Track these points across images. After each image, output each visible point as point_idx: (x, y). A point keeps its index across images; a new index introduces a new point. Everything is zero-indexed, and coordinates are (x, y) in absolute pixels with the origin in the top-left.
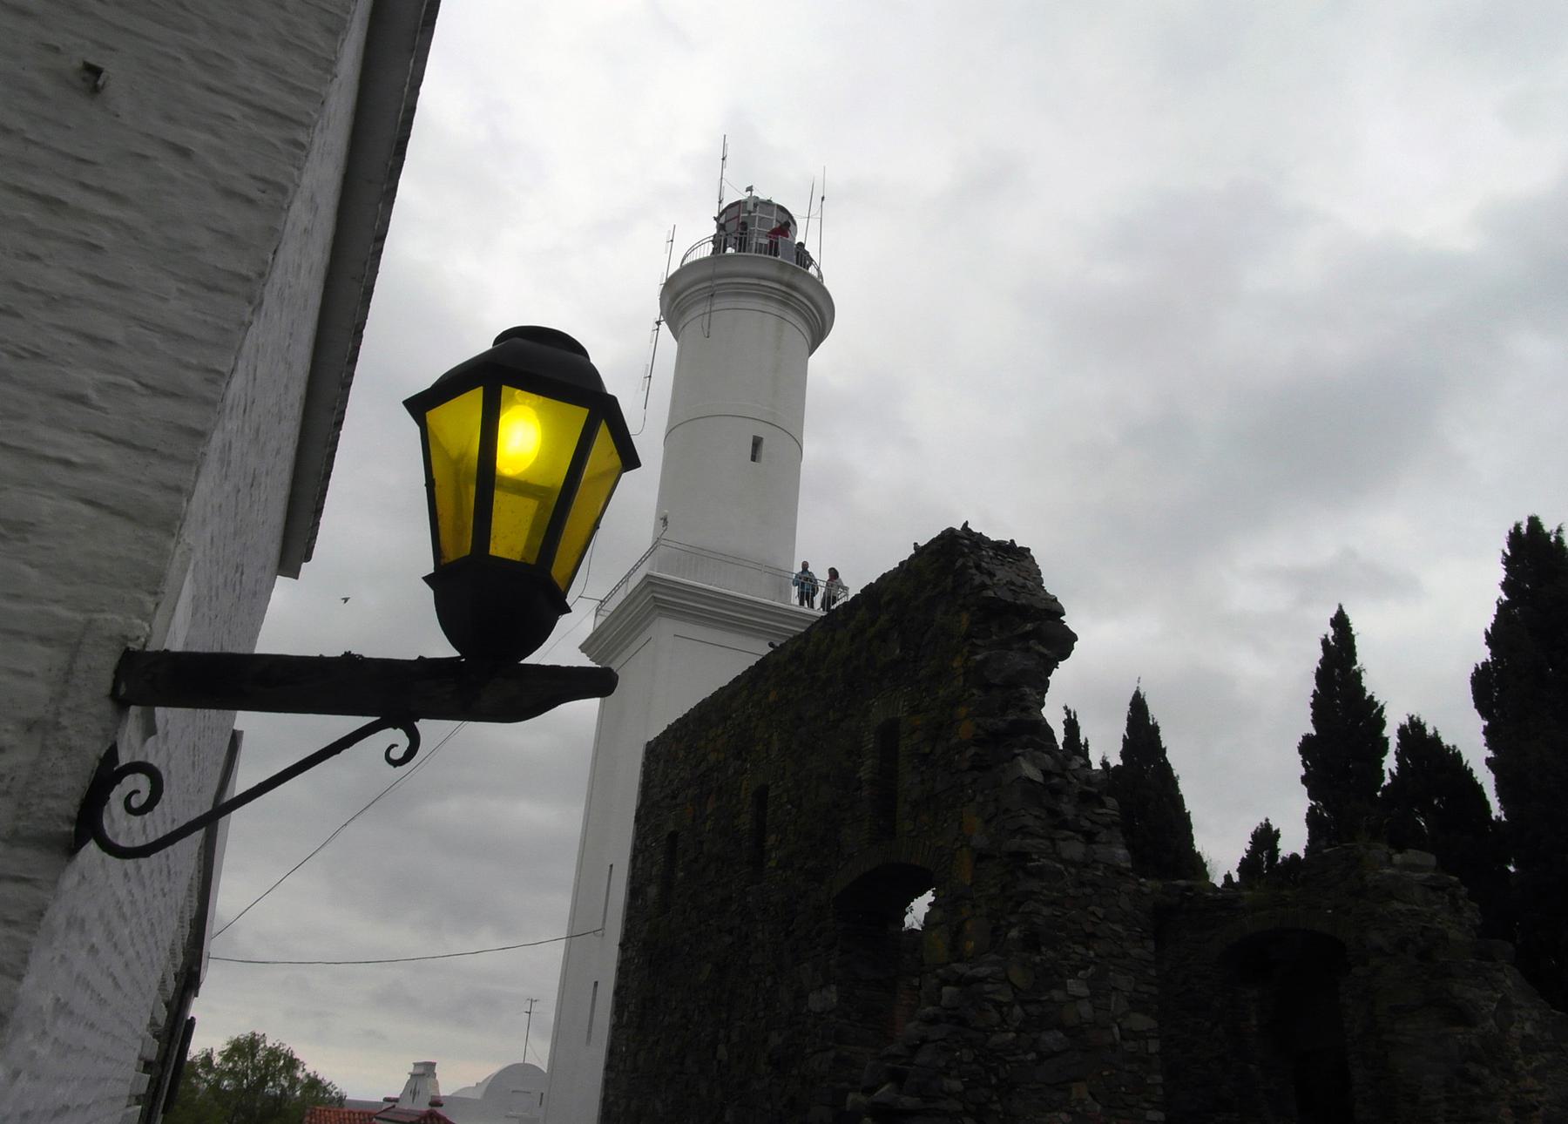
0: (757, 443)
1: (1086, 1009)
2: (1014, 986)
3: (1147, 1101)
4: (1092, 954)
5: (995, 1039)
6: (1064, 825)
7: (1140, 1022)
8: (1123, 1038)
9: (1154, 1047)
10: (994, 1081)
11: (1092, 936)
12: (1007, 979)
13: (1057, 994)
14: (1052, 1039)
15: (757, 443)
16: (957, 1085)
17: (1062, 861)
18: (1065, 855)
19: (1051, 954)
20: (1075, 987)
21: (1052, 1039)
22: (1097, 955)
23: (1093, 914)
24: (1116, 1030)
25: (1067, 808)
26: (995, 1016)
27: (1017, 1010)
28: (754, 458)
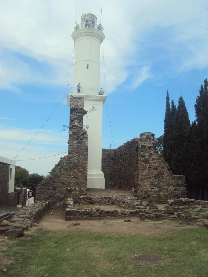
0: (88, 65)
1: (76, 161)
5: (63, 165)
11: (78, 152)
13: (72, 159)
14: (71, 165)
15: (88, 65)
16: (57, 170)
18: (74, 143)
19: (72, 155)
21: (71, 165)
24: (81, 163)
26: (63, 162)
28: (88, 68)
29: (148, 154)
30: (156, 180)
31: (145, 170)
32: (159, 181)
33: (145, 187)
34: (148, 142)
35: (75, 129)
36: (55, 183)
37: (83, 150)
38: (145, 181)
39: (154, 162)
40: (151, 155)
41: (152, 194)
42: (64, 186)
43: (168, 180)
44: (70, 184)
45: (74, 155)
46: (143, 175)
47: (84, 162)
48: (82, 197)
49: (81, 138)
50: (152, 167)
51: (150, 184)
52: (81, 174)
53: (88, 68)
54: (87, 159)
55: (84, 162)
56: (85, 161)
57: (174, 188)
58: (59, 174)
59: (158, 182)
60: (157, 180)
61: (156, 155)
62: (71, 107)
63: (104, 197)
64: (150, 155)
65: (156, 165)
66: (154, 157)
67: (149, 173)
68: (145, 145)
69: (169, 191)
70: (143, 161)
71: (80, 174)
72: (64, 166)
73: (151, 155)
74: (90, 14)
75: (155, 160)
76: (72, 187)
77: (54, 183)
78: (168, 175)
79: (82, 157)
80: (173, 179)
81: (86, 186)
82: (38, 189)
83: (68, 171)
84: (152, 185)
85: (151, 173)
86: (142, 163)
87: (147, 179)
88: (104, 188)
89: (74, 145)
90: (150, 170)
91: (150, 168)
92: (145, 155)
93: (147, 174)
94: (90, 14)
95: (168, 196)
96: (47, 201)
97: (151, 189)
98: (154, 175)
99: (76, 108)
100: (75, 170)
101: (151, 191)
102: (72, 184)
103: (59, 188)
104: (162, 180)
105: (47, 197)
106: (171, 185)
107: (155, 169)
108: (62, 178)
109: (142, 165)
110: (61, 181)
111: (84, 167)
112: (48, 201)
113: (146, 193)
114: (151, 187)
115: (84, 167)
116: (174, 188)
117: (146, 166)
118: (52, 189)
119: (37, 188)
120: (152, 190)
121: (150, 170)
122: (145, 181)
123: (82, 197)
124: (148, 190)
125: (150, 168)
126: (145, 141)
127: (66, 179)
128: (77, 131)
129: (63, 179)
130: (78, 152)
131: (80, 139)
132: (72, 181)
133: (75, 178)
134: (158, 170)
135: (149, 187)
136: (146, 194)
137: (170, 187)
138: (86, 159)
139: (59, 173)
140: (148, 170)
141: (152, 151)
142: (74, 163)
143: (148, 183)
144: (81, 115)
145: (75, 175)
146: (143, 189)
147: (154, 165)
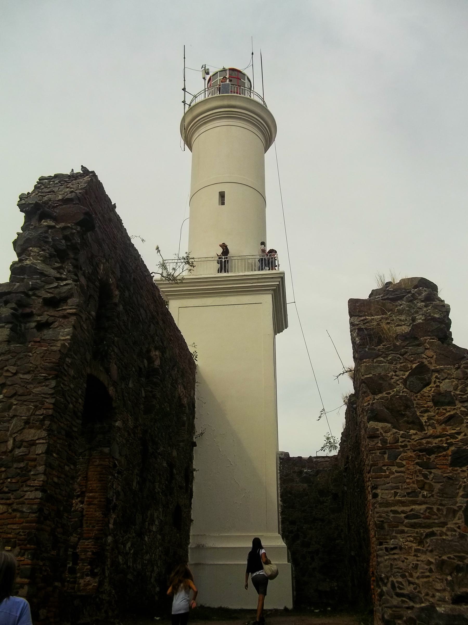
7: (31, 434)
9: (40, 449)
22: (5, 397)
23: (7, 371)
24: (11, 442)
29: (405, 369)
31: (394, 469)
33: (409, 589)
34: (400, 312)
37: (29, 373)
38: (401, 540)
39: (451, 418)
40: (421, 374)
46: (387, 504)
49: (39, 318)
50: (439, 448)
51: (441, 565)
56: (33, 431)
64: (414, 372)
66: (445, 386)
67: (422, 488)
70: (376, 417)
73: (421, 374)
75: (452, 403)
84: (458, 569)
85: (438, 486)
87: (413, 526)
90: (426, 465)
92: (383, 378)
93: (413, 493)
109: (373, 436)
111: (22, 465)
114: (450, 584)
115: (22, 465)
117: (397, 441)
121: (426, 465)
122: (401, 540)
124: (432, 607)
125: (430, 451)
131: (33, 324)
135: (439, 586)
141: (430, 353)
143: (423, 557)
146: (396, 601)
147: (452, 436)
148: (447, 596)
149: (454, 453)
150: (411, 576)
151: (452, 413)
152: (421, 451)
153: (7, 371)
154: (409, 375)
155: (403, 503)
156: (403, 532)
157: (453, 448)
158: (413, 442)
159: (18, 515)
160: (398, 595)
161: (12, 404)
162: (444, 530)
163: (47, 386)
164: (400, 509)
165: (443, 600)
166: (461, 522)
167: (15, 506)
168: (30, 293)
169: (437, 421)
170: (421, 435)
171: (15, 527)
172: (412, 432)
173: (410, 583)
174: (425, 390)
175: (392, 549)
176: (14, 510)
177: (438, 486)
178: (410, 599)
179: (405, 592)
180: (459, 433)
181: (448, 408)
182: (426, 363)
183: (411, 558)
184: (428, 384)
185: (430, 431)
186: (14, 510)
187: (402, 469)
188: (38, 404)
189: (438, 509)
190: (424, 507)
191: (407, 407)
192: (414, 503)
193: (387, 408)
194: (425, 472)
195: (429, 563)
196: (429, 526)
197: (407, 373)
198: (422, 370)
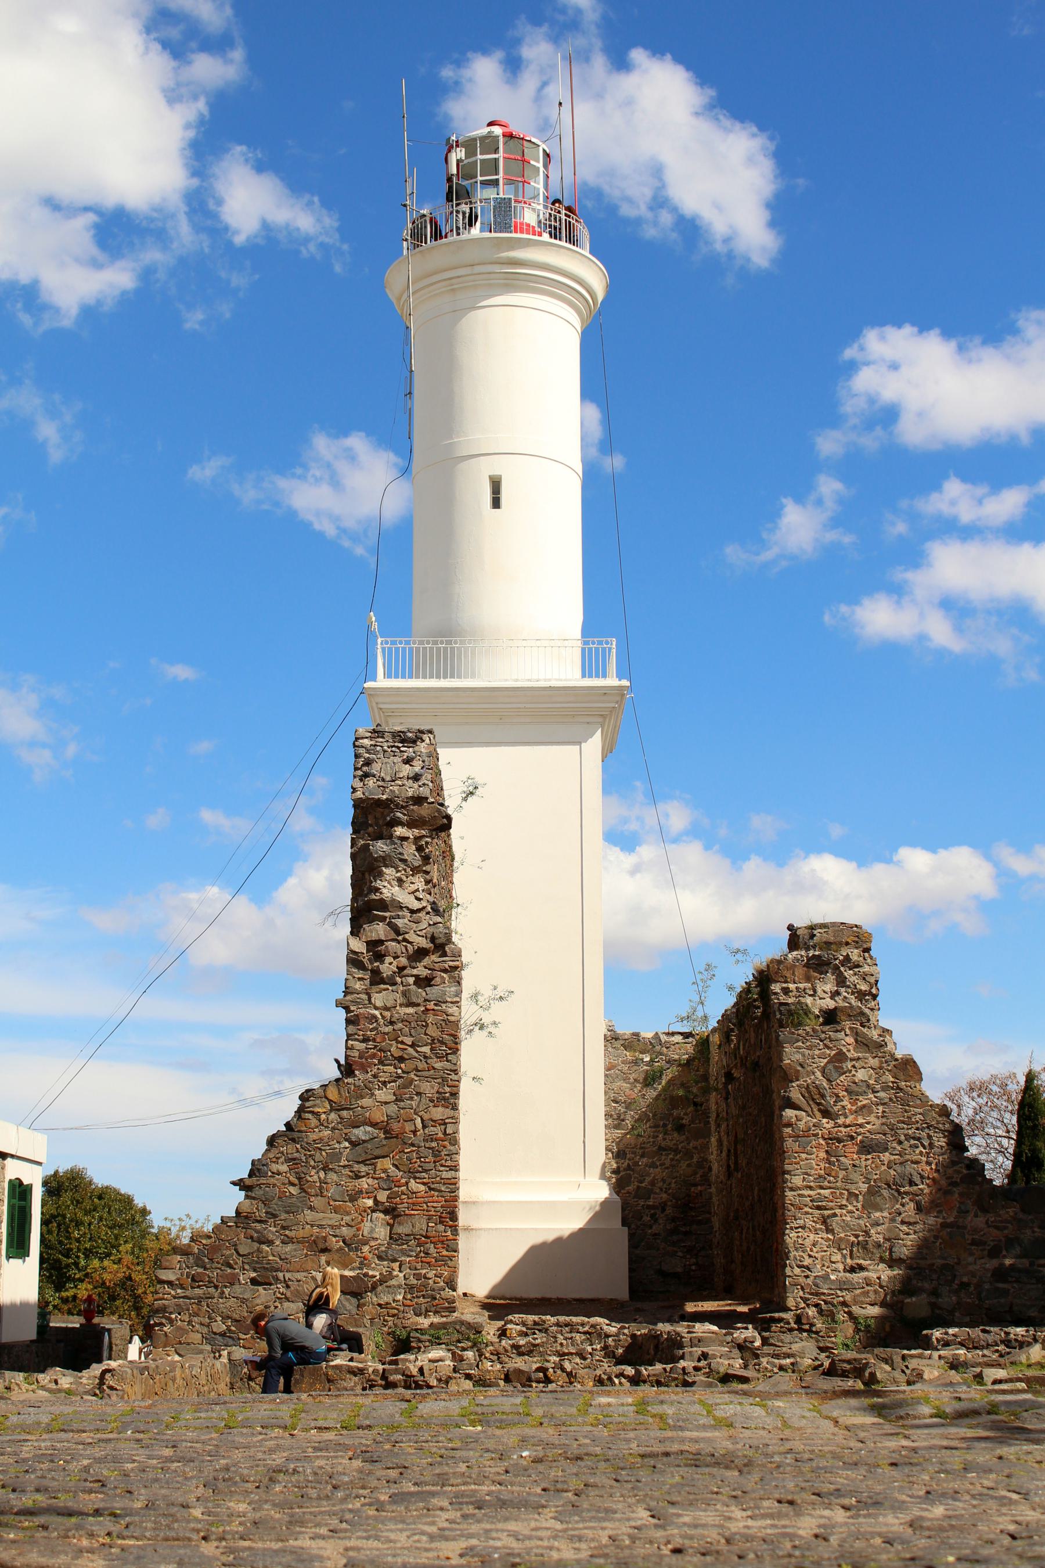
1: (392, 1109)
2: (330, 1101)
3: (442, 1166)
4: (399, 1071)
6: (383, 981)
8: (424, 1127)
10: (312, 1163)
11: (401, 1059)
12: (326, 1097)
13: (366, 1102)
14: (361, 1133)
15: (496, 486)
16: (284, 1168)
17: (376, 1008)
18: (379, 1004)
20: (382, 1095)
21: (361, 1133)
23: (402, 1043)
24: (419, 1120)
25: (387, 968)
26: (314, 1122)
27: (333, 1116)
28: (496, 503)
30: (878, 1214)
31: (804, 1156)
32: (893, 1220)
33: (807, 1261)
35: (383, 919)
36: (270, 1243)
41: (856, 1303)
42: (323, 1259)
43: (955, 1213)
44: (357, 1249)
45: (375, 1076)
47: (438, 1113)
48: (424, 1322)
49: (415, 972)
52: (422, 1188)
53: (496, 503)
54: (455, 1095)
55: (438, 1113)
56: (440, 1109)
57: (992, 1264)
58: (294, 1190)
59: (889, 1230)
60: (886, 1214)
61: (874, 1062)
62: (354, 790)
63: (558, 1324)
65: (872, 1124)
66: (861, 1075)
68: (809, 1000)
69: (964, 1285)
71: (413, 1185)
72: (321, 1139)
74: (497, 131)
76: (368, 1266)
77: (265, 1247)
78: (954, 1184)
79: (429, 1088)
80: (985, 1210)
81: (450, 1258)
82: (170, 1283)
83: (346, 1171)
85: (842, 1174)
86: (789, 1113)
87: (819, 1208)
88: (622, 1292)
89: (374, 1017)
91: (839, 1141)
94: (497, 131)
95: (957, 1314)
96: (225, 1353)
97: (852, 1270)
98: (864, 1187)
99: (384, 797)
100: (386, 1163)
101: (843, 1285)
102: (366, 1249)
103: (288, 1275)
104: (912, 1213)
105: (219, 1326)
106: (974, 1243)
107: (867, 1148)
108: (309, 1215)
110: (301, 1233)
111: (434, 1144)
112: (229, 1353)
113: (817, 1294)
114: (844, 1256)
115: (434, 1144)
116: (992, 1264)
118: (254, 1282)
119: (164, 1278)
120: (857, 1277)
123: (424, 1322)
124: (826, 1277)
125: (839, 1141)
126: (808, 979)
127: (334, 1218)
128: (393, 935)
129: (317, 1218)
130: (401, 1059)
131: (411, 980)
132: (366, 1227)
133: (386, 1212)
134: (886, 1157)
136: (815, 1300)
137: (971, 1259)
138: (449, 1098)
139: (294, 1185)
140: (822, 1155)
142: (374, 1125)
144: (417, 839)
145: (382, 1196)
146: (797, 1271)
147: (861, 1126)
148: (841, 1267)
149: (862, 1142)
150: (811, 1250)
151: (865, 1102)
152: (831, 1139)
153: (402, 1043)
154: (828, 1062)
155: (811, 1188)
156: (807, 1213)
157: (860, 1138)
158: (825, 1131)
159: (436, 1194)
160: (799, 1266)
161: (412, 1080)
162: (844, 1211)
163: (448, 1061)
164: (806, 1192)
165: (835, 1270)
166: (859, 1206)
167: (432, 1186)
168: (400, 938)
169: (850, 1110)
170: (832, 1123)
171: (435, 1204)
172: (825, 1120)
173: (810, 1256)
174: (842, 1078)
175: (797, 1228)
176: (431, 1189)
177: (842, 1174)
178: (809, 1269)
179: (805, 1263)
180: (868, 1123)
181: (861, 1098)
182: (845, 1050)
183: (812, 1236)
184: (845, 1073)
185: (840, 1121)
186: (431, 1189)
187: (813, 1156)
188: (440, 1080)
189: (841, 1194)
190: (829, 1191)
191: (823, 1096)
192: (822, 1188)
193: (804, 1097)
194: (833, 1159)
195: (828, 1239)
196: (832, 1209)
197: (826, 1061)
198: (841, 1057)
